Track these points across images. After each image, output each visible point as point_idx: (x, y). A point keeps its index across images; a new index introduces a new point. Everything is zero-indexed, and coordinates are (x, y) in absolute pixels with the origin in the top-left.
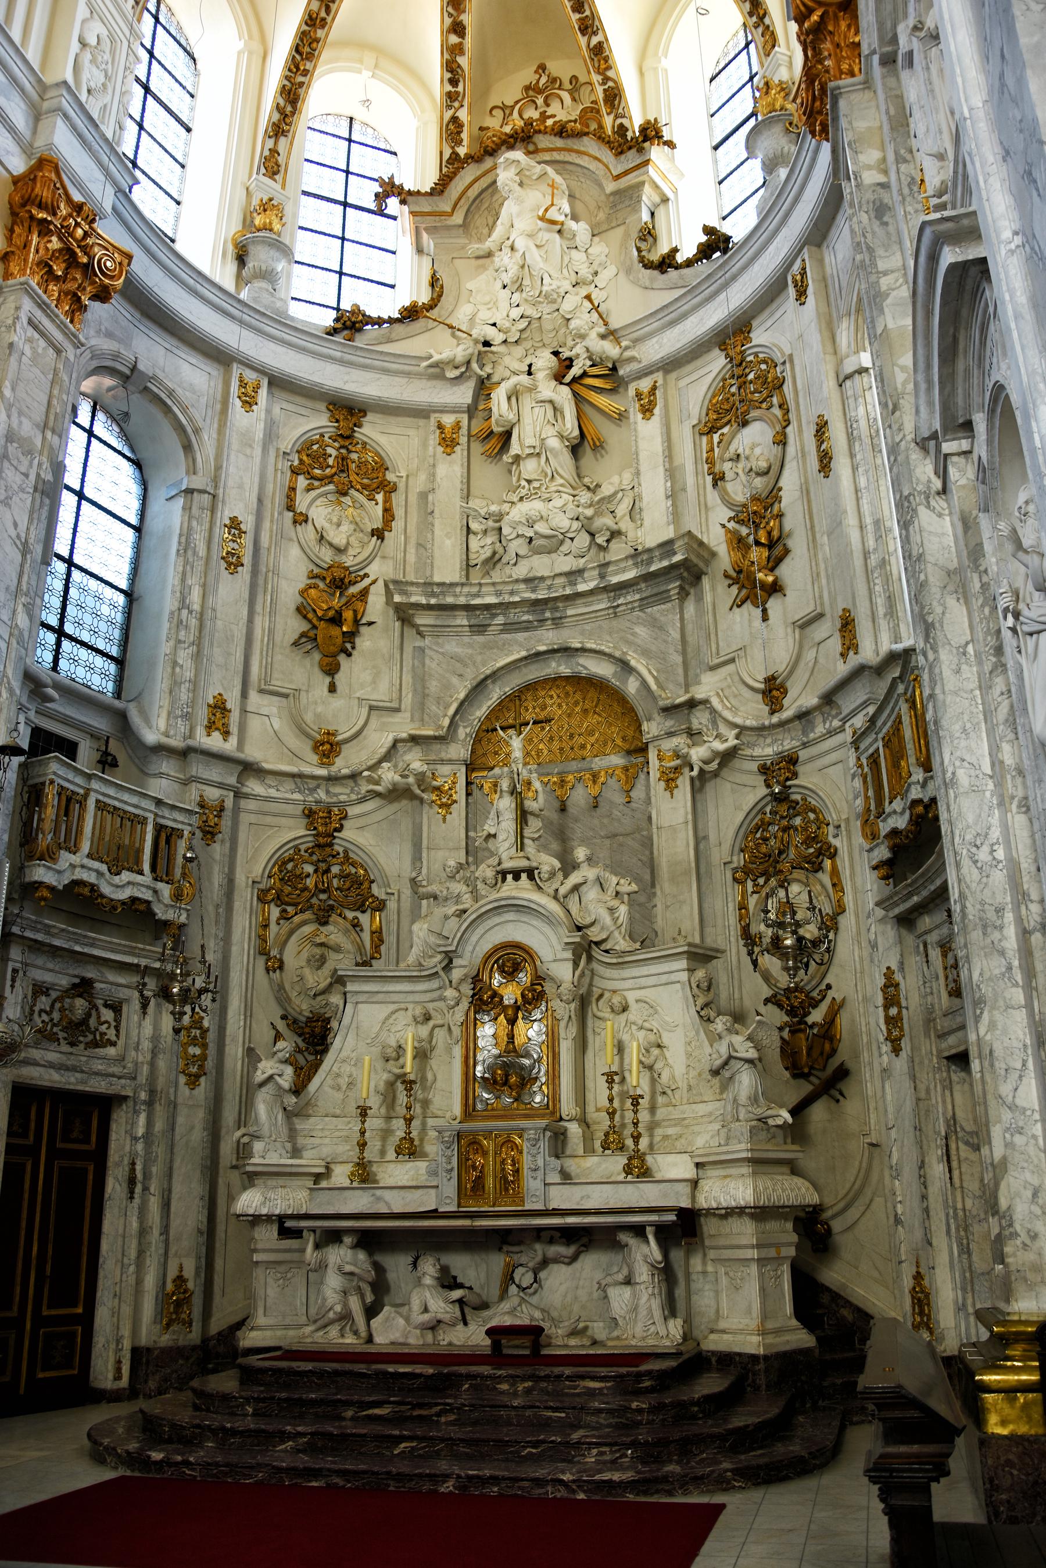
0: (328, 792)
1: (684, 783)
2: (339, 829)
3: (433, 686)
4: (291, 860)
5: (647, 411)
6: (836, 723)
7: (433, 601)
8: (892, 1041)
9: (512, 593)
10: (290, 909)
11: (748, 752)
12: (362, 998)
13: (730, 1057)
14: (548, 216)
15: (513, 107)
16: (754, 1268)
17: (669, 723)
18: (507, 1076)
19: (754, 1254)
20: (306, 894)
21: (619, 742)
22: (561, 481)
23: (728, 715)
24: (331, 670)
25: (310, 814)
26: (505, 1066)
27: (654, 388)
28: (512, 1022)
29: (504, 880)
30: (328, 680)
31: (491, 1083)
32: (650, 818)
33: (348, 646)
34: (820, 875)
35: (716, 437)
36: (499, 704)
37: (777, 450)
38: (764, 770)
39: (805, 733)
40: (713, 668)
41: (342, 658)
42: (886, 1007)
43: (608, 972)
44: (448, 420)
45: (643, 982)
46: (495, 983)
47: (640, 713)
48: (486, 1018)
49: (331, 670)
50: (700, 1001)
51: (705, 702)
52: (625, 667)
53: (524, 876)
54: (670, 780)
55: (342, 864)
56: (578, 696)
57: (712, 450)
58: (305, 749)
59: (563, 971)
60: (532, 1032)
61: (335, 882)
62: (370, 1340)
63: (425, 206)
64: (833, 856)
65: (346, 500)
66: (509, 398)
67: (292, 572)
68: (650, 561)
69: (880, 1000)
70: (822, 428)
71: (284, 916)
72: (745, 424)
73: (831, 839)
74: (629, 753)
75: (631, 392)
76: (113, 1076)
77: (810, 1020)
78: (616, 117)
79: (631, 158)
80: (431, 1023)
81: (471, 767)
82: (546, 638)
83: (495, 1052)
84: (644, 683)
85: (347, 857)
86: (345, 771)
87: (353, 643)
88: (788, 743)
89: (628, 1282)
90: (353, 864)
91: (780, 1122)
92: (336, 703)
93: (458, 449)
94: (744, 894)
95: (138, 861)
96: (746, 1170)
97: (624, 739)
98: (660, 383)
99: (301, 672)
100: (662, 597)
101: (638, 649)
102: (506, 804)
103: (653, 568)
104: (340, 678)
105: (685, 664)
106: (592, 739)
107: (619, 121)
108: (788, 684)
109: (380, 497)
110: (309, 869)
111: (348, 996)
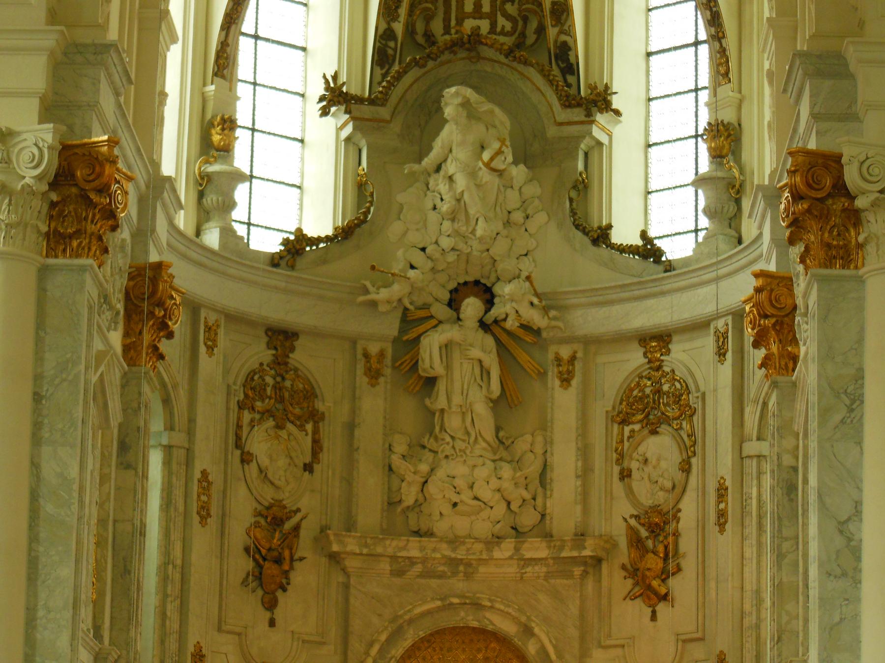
3: (356, 624)
5: (566, 380)
7: (365, 551)
14: (493, 165)
22: (484, 445)
24: (271, 604)
27: (573, 359)
30: (268, 615)
33: (284, 581)
35: (627, 430)
36: (413, 645)
37: (679, 476)
41: (279, 594)
49: (271, 604)
52: (528, 631)
57: (622, 441)
63: (366, 111)
65: (283, 434)
66: (440, 348)
72: (654, 432)
75: (551, 356)
78: (561, 32)
79: (577, 114)
84: (543, 648)
87: (287, 578)
93: (382, 380)
98: (579, 355)
99: (247, 607)
103: (564, 554)
104: (279, 613)
105: (582, 639)
107: (563, 38)
109: (309, 427)
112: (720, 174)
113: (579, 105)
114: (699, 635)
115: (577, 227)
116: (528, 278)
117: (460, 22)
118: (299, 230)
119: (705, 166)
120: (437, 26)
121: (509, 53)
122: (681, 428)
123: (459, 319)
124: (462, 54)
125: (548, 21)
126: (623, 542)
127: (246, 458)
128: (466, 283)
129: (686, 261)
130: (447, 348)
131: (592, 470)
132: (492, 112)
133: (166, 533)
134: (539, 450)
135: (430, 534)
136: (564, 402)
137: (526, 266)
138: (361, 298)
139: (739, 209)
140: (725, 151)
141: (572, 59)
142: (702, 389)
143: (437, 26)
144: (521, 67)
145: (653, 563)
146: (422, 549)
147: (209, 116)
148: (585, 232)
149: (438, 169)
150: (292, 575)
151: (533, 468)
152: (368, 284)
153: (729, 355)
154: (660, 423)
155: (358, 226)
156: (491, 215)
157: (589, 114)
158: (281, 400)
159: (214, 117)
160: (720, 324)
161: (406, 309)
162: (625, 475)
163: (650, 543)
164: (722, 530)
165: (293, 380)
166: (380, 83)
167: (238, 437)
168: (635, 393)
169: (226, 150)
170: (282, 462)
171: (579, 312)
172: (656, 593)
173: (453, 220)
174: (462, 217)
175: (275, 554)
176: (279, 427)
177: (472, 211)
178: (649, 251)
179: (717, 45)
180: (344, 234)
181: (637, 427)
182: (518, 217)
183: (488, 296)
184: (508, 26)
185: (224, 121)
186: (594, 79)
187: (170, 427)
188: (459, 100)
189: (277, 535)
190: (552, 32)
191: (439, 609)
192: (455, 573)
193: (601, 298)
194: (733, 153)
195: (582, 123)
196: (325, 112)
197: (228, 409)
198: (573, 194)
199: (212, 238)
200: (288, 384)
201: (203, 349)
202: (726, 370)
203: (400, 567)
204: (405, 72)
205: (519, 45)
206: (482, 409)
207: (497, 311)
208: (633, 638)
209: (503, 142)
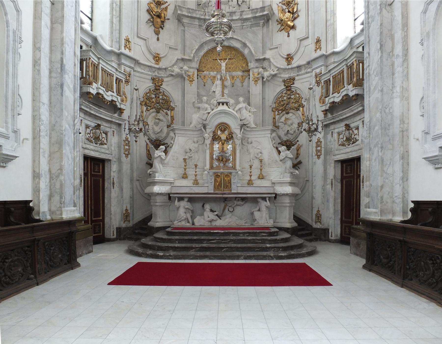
0: (158, 73)
1: (260, 82)
2: (161, 85)
3: (188, 43)
4: (149, 93)
6: (309, 70)
7: (189, 15)
8: (318, 156)
10: (149, 108)
11: (279, 75)
12: (180, 135)
13: (286, 157)
16: (288, 208)
18: (223, 158)
19: (288, 205)
20: (153, 103)
21: (241, 68)
23: (275, 64)
24: (157, 33)
25: (153, 79)
26: (222, 156)
28: (223, 144)
29: (219, 105)
30: (157, 36)
31: (218, 160)
32: (249, 92)
33: (162, 26)
34: (298, 112)
38: (284, 81)
39: (298, 72)
40: (270, 49)
41: (160, 29)
42: (317, 147)
43: (247, 133)
46: (219, 133)
47: (248, 60)
48: (216, 143)
49: (157, 33)
50: (273, 142)
51: (268, 59)
52: (245, 45)
53: (225, 104)
54: (256, 82)
55: (162, 96)
56: (229, 52)
58: (151, 58)
60: (229, 147)
61: (161, 101)
62: (193, 224)
64: (303, 107)
68: (256, 13)
69: (315, 145)
71: (147, 110)
73: (303, 102)
74: (243, 71)
76: (107, 154)
80: (198, 143)
81: (198, 70)
83: (218, 152)
85: (164, 94)
86: (164, 67)
88: (292, 75)
89: (259, 210)
90: (165, 96)
91: (296, 174)
94: (275, 115)
95: (112, 88)
96: (288, 185)
100: (257, 25)
103: (257, 15)
104: (160, 36)
106: (233, 66)
108: (294, 57)
110: (153, 96)
111: (176, 134)
150: (165, 24)
208: (281, 44)
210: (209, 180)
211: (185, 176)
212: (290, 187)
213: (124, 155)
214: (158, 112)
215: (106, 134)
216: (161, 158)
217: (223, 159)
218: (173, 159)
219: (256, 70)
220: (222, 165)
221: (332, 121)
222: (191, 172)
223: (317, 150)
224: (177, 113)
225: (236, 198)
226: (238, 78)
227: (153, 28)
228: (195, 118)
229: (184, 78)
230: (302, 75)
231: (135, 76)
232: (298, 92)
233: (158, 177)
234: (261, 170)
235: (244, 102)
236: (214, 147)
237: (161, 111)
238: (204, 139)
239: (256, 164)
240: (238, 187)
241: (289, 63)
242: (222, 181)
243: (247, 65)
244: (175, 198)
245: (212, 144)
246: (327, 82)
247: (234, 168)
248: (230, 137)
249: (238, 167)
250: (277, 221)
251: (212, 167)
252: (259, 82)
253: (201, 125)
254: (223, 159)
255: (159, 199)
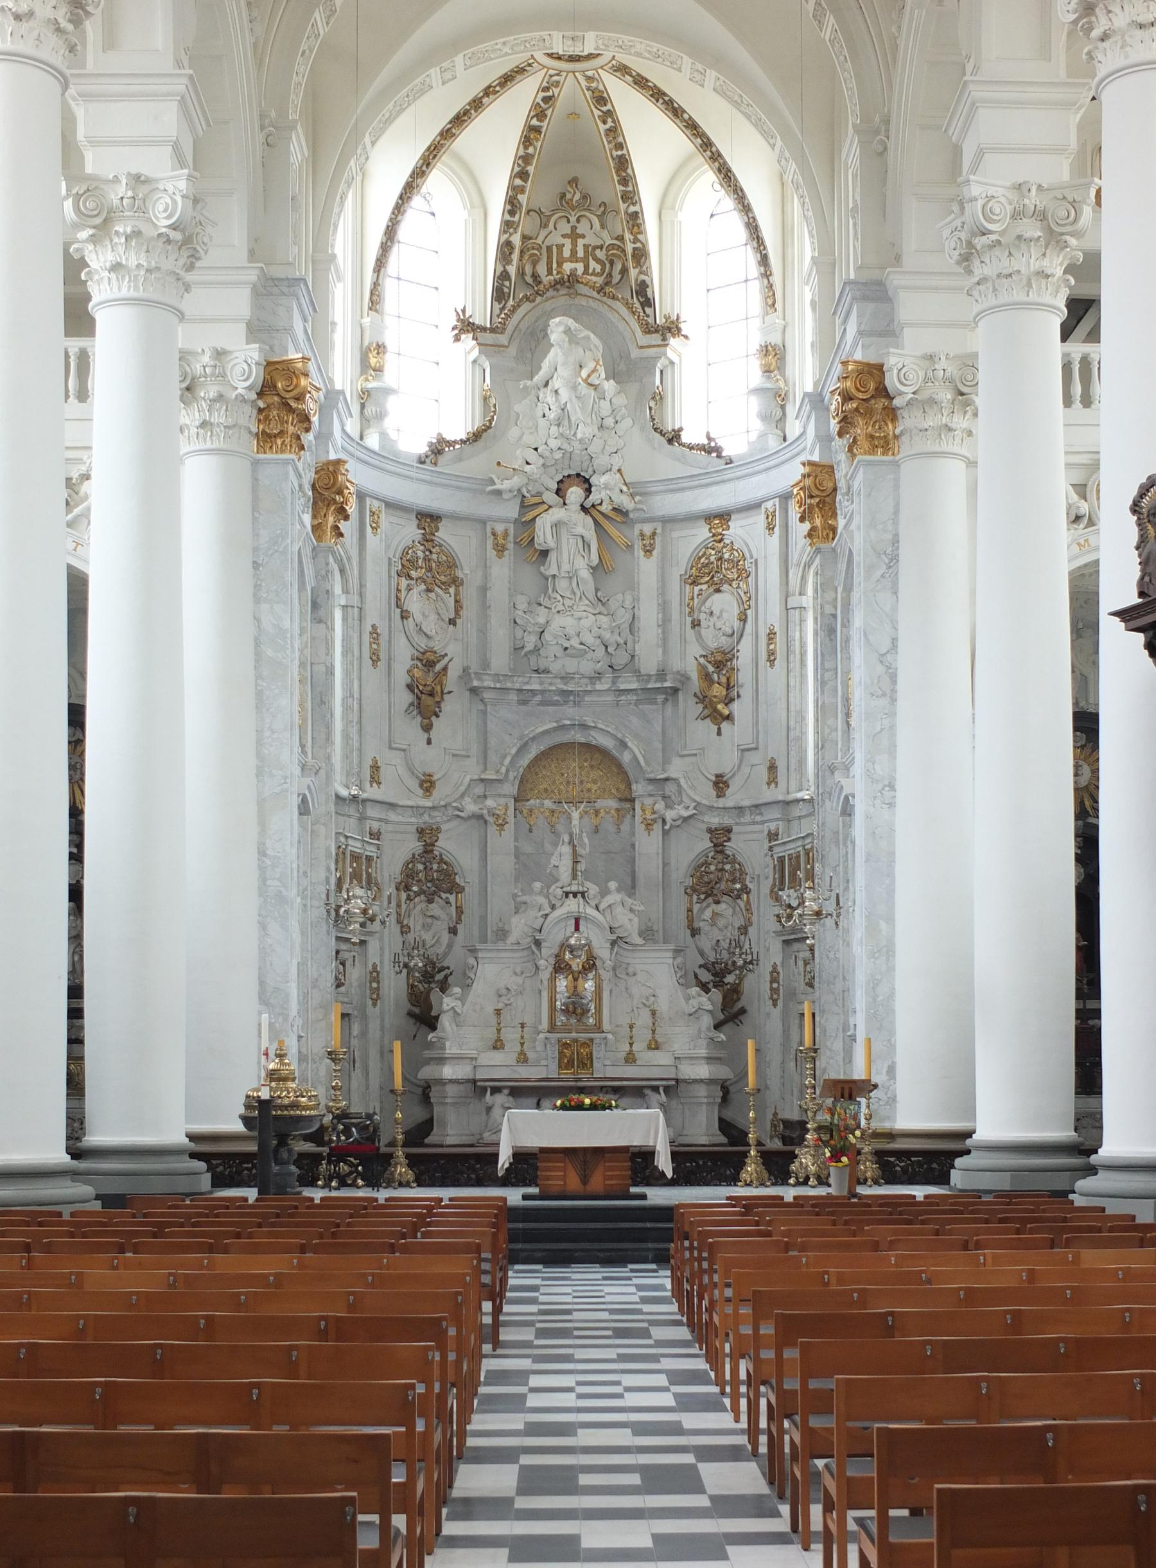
1: (657, 827)
3: (492, 741)
5: (648, 552)
6: (758, 818)
7: (498, 686)
9: (550, 684)
15: (550, 216)
17: (651, 787)
19: (705, 1100)
24: (427, 728)
25: (421, 832)
26: (573, 1003)
27: (654, 534)
28: (576, 979)
29: (567, 896)
30: (426, 736)
31: (566, 1011)
32: (633, 846)
34: (739, 901)
35: (697, 589)
37: (737, 624)
38: (710, 831)
41: (433, 718)
43: (625, 953)
44: (500, 528)
45: (646, 961)
47: (631, 777)
49: (427, 728)
52: (623, 745)
53: (579, 896)
54: (649, 826)
57: (693, 599)
58: (414, 784)
59: (602, 951)
63: (488, 337)
64: (748, 893)
65: (432, 595)
67: (403, 656)
68: (648, 681)
69: (768, 978)
70: (771, 636)
71: (409, 898)
72: (718, 591)
74: (621, 800)
75: (637, 532)
77: (726, 980)
78: (641, 273)
79: (655, 339)
81: (516, 800)
82: (570, 713)
84: (635, 758)
88: (727, 821)
90: (446, 863)
92: (432, 751)
94: (691, 903)
97: (617, 790)
99: (410, 730)
100: (653, 702)
101: (635, 737)
102: (566, 850)
105: (664, 749)
107: (643, 277)
108: (730, 783)
109: (452, 590)
110: (420, 867)
112: (769, 386)
113: (657, 331)
114: (753, 746)
115: (656, 430)
116: (619, 470)
117: (560, 264)
118: (439, 434)
119: (756, 378)
120: (542, 269)
121: (600, 290)
122: (738, 587)
123: (565, 504)
124: (563, 291)
125: (630, 264)
126: (694, 675)
127: (405, 615)
128: (569, 476)
129: (742, 457)
130: (556, 525)
131: (670, 621)
132: (588, 338)
133: (347, 673)
134: (628, 604)
135: (547, 671)
136: (647, 568)
137: (616, 462)
138: (490, 488)
139: (784, 414)
140: (772, 368)
141: (649, 295)
142: (755, 556)
143: (542, 269)
144: (610, 302)
145: (718, 691)
146: (541, 683)
147: (366, 343)
148: (662, 434)
149: (546, 384)
150: (443, 705)
151: (624, 617)
152: (494, 476)
153: (777, 529)
154: (722, 582)
155: (485, 430)
156: (589, 421)
157: (664, 339)
158: (430, 569)
159: (370, 344)
160: (769, 505)
161: (524, 496)
162: (696, 624)
163: (715, 676)
164: (772, 666)
165: (438, 554)
166: (498, 316)
167: (398, 599)
168: (702, 560)
169: (379, 370)
170: (433, 617)
171: (658, 498)
172: (721, 714)
173: (558, 425)
174: (566, 423)
175: (429, 688)
176: (429, 590)
177: (573, 419)
178: (711, 449)
179: (766, 281)
180: (476, 437)
181: (704, 587)
182: (609, 422)
183: (586, 486)
184: (598, 268)
185: (378, 346)
186: (667, 310)
187: (346, 591)
188: (561, 329)
189: (431, 674)
190: (633, 272)
191: (555, 729)
192: (566, 702)
193: (674, 485)
194: (779, 368)
195: (659, 346)
196: (457, 339)
197: (390, 577)
198: (652, 404)
199: (373, 441)
200: (434, 556)
201: (369, 529)
202: (774, 541)
203: (525, 697)
204: (519, 306)
205: (607, 283)
206: (585, 574)
207: (594, 497)
209: (598, 362)
210: (549, 1052)
211: (498, 1045)
212: (706, 1067)
213: (371, 1002)
214: (430, 901)
215: (343, 964)
216: (455, 1012)
217: (575, 1009)
218: (475, 1011)
219: (648, 801)
220: (573, 1021)
221: (792, 937)
222: (511, 1036)
223: (772, 989)
224: (470, 898)
225: (602, 1087)
226: (608, 813)
227: (419, 719)
228: (519, 926)
229: (486, 822)
230: (745, 824)
231: (387, 832)
232: (739, 859)
233: (451, 1049)
234: (654, 1031)
235: (618, 890)
236: (558, 984)
237: (436, 898)
238: (537, 968)
239: (644, 1018)
240: (607, 1066)
241: (720, 794)
242: (576, 1056)
243: (629, 785)
244: (484, 1089)
245: (553, 980)
246: (781, 860)
247: (598, 1028)
248: (590, 965)
249: (606, 1026)
250: (685, 1133)
251: (552, 1028)
252: (655, 827)
253: (529, 939)
254: (575, 1009)
255: (450, 1090)
